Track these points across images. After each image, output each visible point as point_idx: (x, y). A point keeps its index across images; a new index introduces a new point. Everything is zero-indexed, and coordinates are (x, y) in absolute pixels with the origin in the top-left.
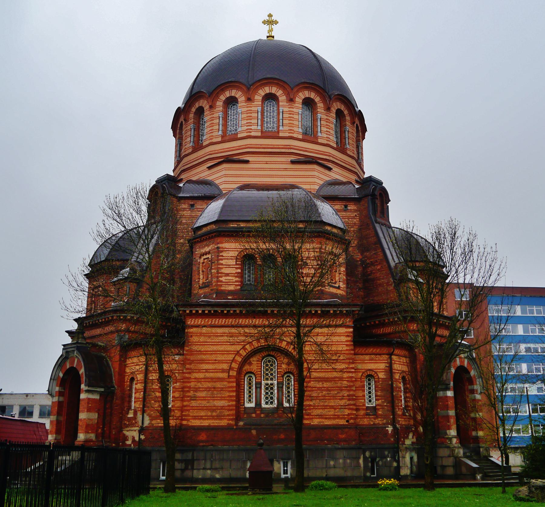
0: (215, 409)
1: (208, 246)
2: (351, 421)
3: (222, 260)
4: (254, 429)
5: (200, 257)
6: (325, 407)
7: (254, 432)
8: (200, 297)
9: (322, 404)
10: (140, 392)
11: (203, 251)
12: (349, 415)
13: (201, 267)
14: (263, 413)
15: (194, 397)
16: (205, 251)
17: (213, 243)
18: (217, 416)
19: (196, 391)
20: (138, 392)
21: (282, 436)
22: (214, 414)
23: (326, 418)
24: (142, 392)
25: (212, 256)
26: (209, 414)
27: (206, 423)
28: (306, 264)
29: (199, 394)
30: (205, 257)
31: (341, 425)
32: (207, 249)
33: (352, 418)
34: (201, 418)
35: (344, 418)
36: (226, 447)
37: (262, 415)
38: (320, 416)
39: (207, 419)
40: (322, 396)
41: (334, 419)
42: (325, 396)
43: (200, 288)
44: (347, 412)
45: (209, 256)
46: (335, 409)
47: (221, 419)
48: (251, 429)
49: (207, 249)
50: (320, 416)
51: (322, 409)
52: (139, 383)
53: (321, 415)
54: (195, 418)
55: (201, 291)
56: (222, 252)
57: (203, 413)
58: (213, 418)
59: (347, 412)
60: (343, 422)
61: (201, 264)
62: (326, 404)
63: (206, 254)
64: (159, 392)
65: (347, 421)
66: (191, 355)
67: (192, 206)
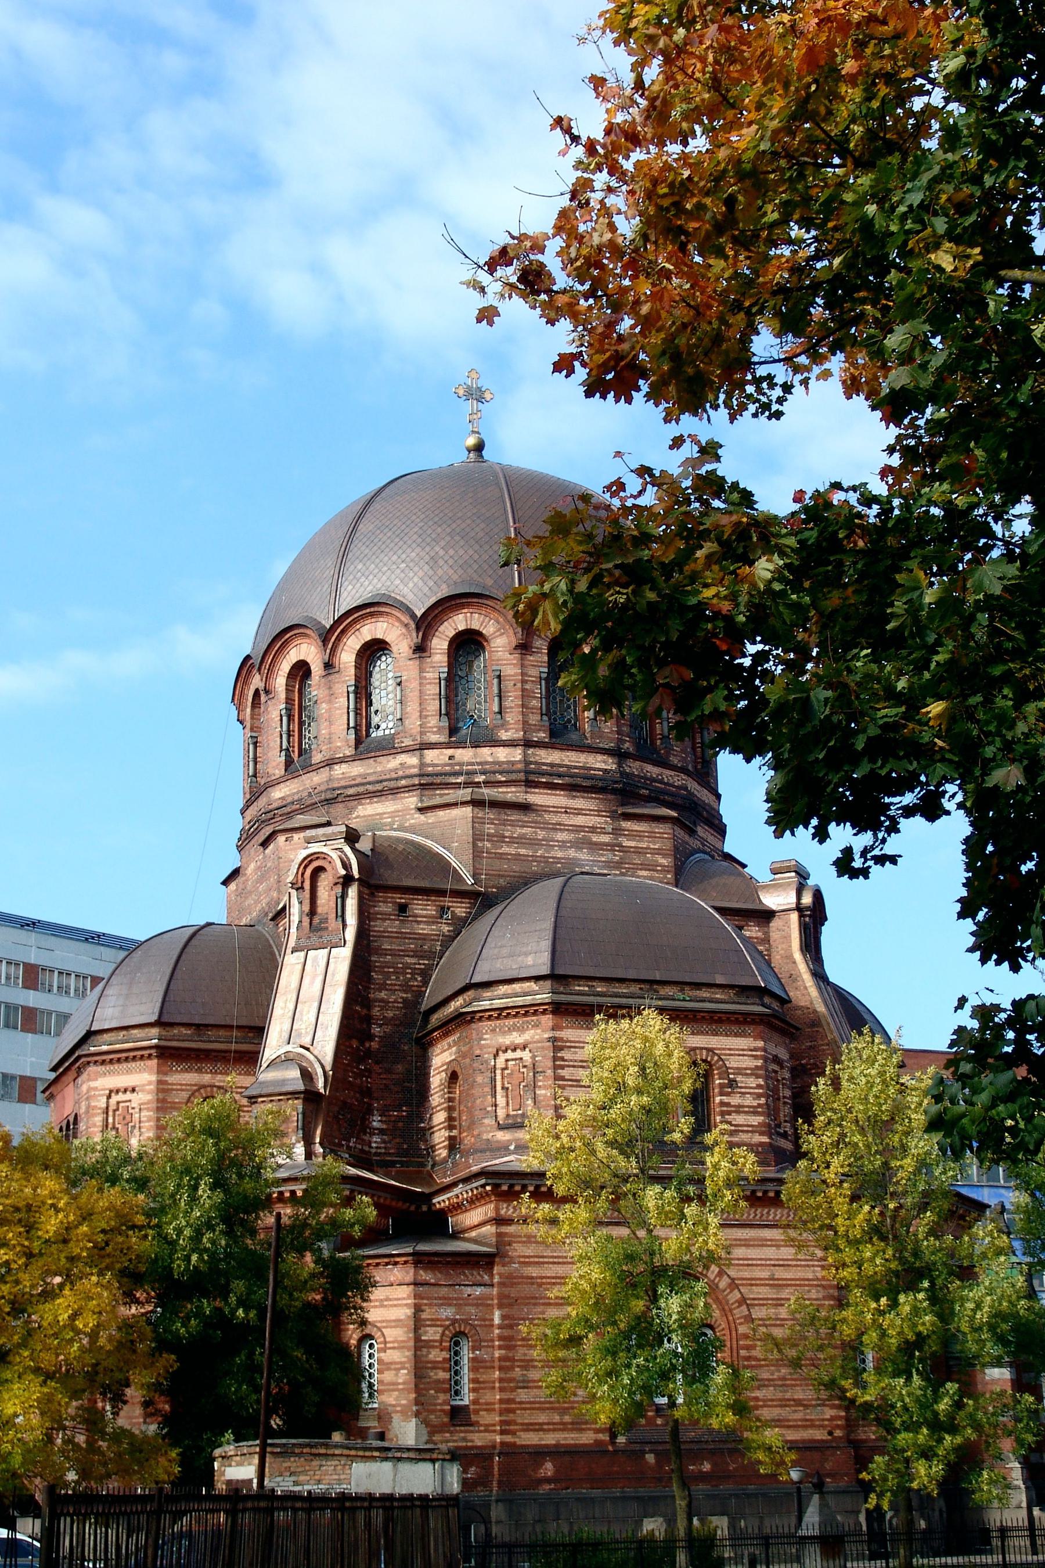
0: (568, 1408)
1: (521, 1030)
2: (838, 1433)
3: (562, 1067)
4: (651, 1451)
5: (496, 1056)
6: (784, 1403)
7: (650, 1458)
8: (507, 1148)
9: (779, 1395)
10: (398, 1370)
11: (507, 1040)
12: (832, 1419)
13: (499, 1077)
14: (660, 1416)
15: (523, 1381)
16: (512, 1043)
17: (536, 1026)
18: (572, 1423)
19: (525, 1368)
20: (389, 1369)
21: (707, 1467)
22: (567, 1418)
23: (789, 1427)
24: (403, 1368)
25: (534, 1057)
26: (557, 1418)
27: (550, 1439)
28: (732, 1084)
29: (534, 1375)
30: (510, 1055)
31: (818, 1441)
32: (517, 1038)
33: (838, 1427)
34: (538, 1428)
35: (823, 1426)
36: (596, 1493)
37: (659, 1421)
38: (778, 1423)
39: (554, 1430)
40: (780, 1379)
41: (805, 1427)
42: (784, 1379)
43: (501, 1127)
44: (829, 1413)
45: (526, 1055)
46: (806, 1406)
47: (581, 1430)
48: (644, 1452)
49: (517, 1038)
50: (778, 1423)
51: (781, 1406)
52: (394, 1348)
53: (779, 1420)
54: (529, 1427)
55: (502, 1136)
56: (561, 1049)
57: (542, 1418)
58: (563, 1427)
59: (829, 1413)
60: (820, 1435)
61: (498, 1072)
62: (788, 1395)
63: (514, 1050)
64: (444, 1370)
65: (830, 1433)
66: (513, 1285)
67: (403, 908)
